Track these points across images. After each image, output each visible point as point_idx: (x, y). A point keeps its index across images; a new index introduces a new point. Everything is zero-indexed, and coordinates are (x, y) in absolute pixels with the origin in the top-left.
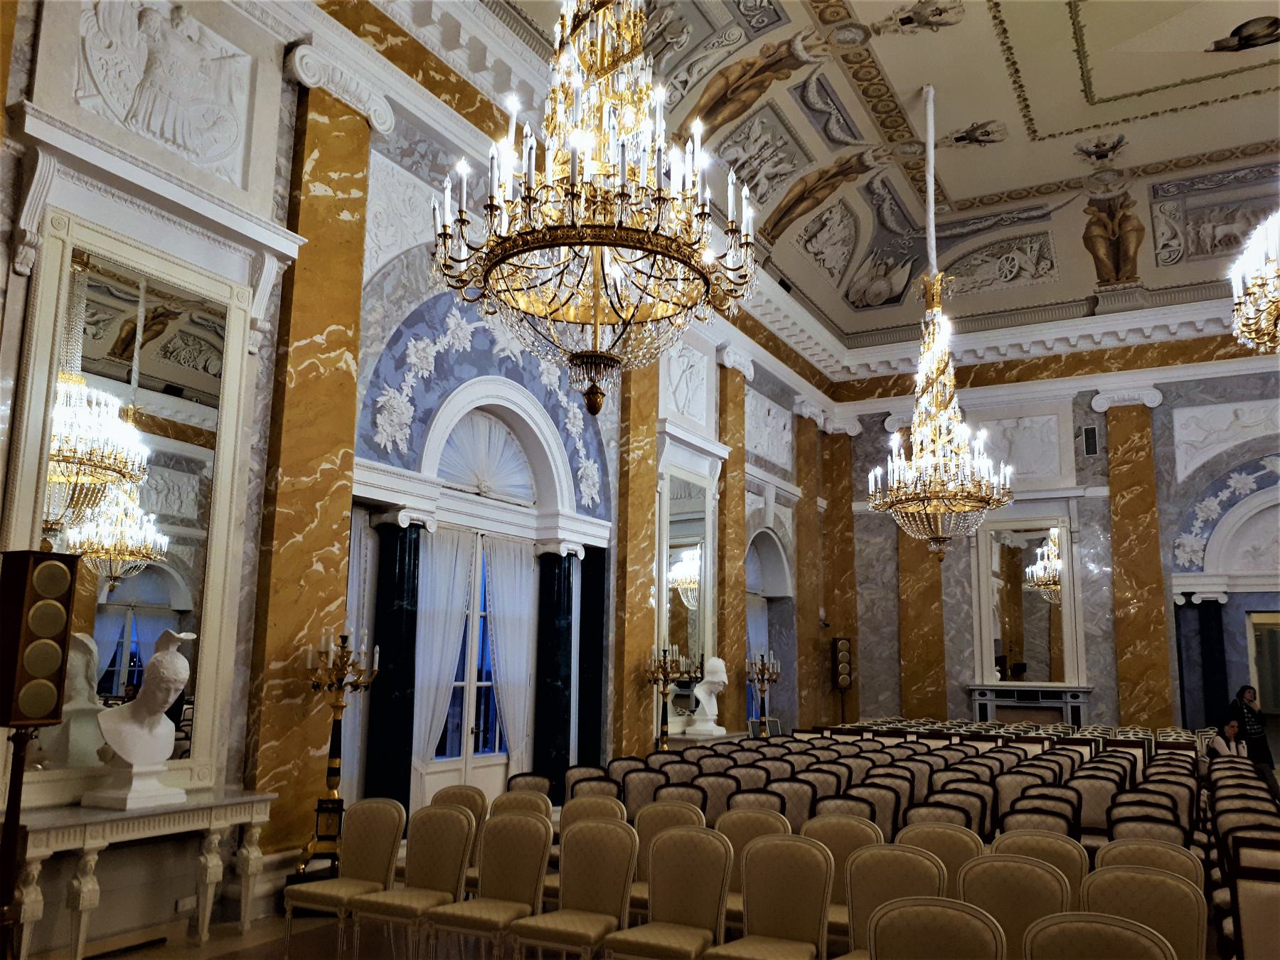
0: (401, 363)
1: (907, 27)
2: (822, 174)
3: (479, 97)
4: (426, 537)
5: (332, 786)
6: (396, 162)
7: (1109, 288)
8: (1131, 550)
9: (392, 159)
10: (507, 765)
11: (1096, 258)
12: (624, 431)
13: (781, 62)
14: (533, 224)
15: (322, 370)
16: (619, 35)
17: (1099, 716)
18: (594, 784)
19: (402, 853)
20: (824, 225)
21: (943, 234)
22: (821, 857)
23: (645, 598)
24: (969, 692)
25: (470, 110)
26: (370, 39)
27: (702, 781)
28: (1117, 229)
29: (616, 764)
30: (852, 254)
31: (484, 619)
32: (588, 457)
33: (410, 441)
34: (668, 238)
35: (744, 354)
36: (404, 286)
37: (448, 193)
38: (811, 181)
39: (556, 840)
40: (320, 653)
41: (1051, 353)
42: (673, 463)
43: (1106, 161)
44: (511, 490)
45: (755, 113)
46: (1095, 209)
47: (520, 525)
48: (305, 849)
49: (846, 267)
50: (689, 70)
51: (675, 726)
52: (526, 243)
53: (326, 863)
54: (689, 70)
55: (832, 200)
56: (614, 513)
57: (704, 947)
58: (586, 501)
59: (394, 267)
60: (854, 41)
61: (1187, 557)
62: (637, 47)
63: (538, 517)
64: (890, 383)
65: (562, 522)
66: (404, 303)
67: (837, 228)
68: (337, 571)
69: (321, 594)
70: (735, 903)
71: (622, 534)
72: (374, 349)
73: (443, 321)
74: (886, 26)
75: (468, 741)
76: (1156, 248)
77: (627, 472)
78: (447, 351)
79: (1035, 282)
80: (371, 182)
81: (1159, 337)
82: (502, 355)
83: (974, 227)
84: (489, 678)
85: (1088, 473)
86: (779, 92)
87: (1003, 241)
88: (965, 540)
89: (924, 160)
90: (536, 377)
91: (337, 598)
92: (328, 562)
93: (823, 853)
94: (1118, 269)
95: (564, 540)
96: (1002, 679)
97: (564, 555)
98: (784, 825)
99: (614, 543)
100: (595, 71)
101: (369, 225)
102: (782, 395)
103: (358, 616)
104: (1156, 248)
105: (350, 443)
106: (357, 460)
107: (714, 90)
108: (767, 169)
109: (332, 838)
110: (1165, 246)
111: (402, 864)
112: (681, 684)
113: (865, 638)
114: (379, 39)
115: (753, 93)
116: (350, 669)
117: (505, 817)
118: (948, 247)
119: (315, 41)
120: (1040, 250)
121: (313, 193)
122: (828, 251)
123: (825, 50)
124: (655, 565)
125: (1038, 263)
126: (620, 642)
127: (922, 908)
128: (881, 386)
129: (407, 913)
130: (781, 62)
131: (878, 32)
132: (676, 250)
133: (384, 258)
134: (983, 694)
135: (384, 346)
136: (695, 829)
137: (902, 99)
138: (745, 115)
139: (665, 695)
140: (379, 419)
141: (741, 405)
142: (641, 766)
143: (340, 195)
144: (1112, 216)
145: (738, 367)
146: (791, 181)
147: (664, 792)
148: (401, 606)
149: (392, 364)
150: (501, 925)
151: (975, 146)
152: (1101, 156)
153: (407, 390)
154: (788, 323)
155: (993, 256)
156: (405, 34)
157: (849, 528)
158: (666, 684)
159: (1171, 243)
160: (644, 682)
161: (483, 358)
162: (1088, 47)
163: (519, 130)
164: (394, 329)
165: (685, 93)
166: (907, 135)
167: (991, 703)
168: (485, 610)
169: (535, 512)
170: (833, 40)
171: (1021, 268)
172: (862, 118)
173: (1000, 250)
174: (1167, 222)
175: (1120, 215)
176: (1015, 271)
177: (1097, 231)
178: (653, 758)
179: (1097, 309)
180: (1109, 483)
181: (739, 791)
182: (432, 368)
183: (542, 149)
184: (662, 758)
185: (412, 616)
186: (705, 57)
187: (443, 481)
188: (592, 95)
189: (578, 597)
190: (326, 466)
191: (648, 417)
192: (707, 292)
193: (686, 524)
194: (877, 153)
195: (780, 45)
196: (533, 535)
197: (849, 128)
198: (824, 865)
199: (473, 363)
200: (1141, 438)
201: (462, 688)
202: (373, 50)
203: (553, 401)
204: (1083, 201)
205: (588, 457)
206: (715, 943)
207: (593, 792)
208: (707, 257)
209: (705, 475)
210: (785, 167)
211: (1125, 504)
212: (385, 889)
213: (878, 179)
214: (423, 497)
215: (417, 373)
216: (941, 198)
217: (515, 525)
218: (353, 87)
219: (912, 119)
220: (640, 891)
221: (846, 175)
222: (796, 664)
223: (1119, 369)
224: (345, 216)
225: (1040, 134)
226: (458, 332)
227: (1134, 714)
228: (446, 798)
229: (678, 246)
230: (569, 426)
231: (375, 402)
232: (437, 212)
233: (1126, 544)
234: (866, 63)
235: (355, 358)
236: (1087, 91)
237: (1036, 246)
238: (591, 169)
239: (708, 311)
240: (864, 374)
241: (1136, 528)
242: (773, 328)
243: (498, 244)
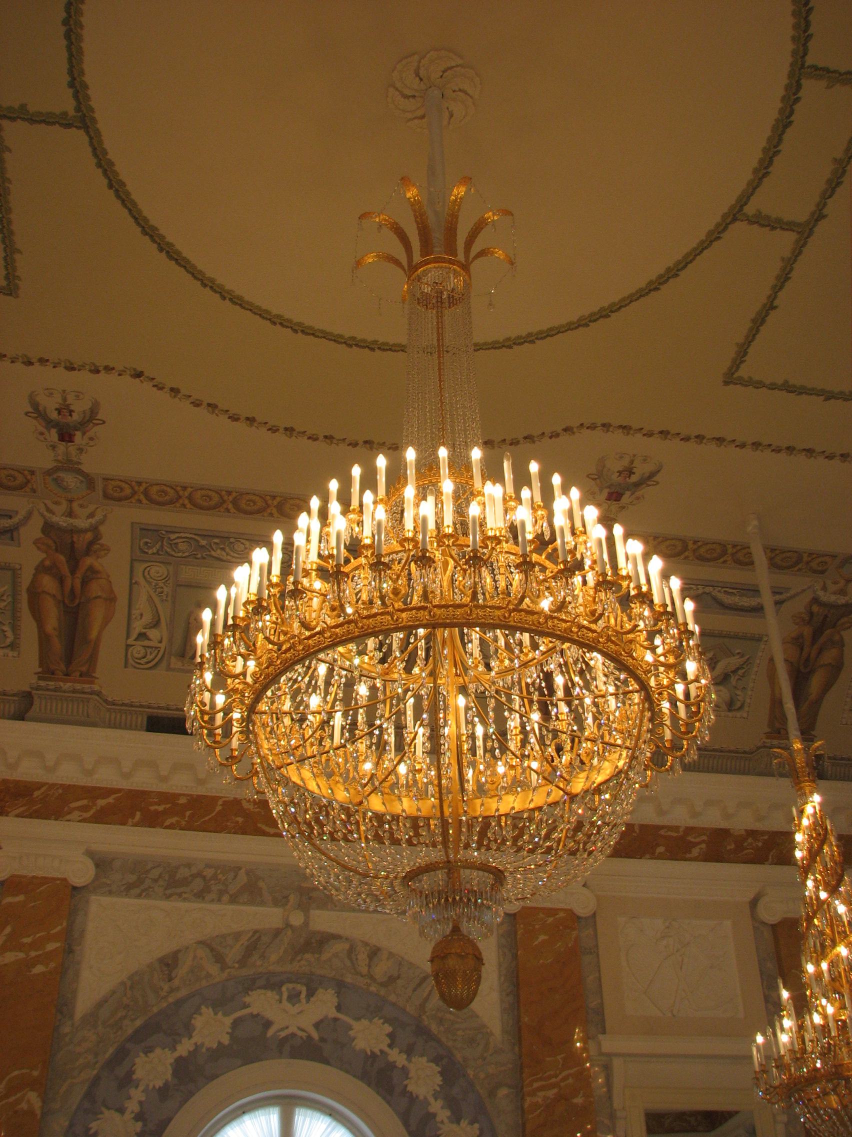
7: (52, 684)
76: (128, 637)
94: (69, 658)
104: (128, 637)
110: (142, 636)
174: (150, 599)
177: (48, 583)
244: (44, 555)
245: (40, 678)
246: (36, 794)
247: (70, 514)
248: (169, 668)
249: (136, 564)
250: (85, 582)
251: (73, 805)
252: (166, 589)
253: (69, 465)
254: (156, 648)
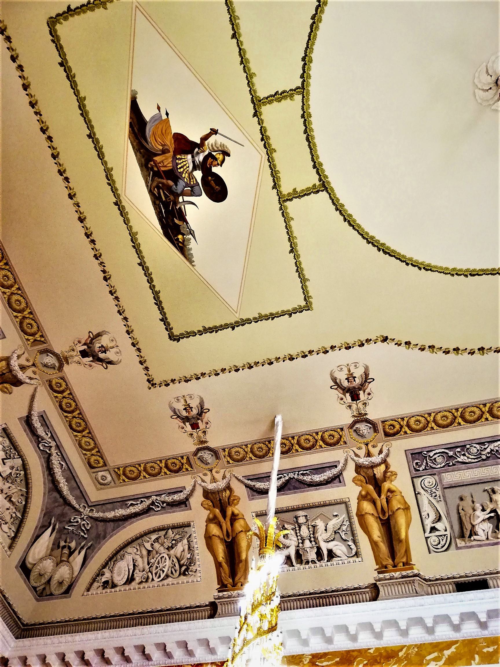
76: (425, 532)
104: (425, 532)
110: (433, 529)
144: (378, 490)
159: (438, 526)
174: (430, 502)
244: (360, 488)
245: (379, 573)
246: (401, 654)
247: (369, 454)
248: (458, 548)
249: (415, 480)
251: (428, 658)
252: (438, 493)
253: (361, 418)
254: (445, 535)
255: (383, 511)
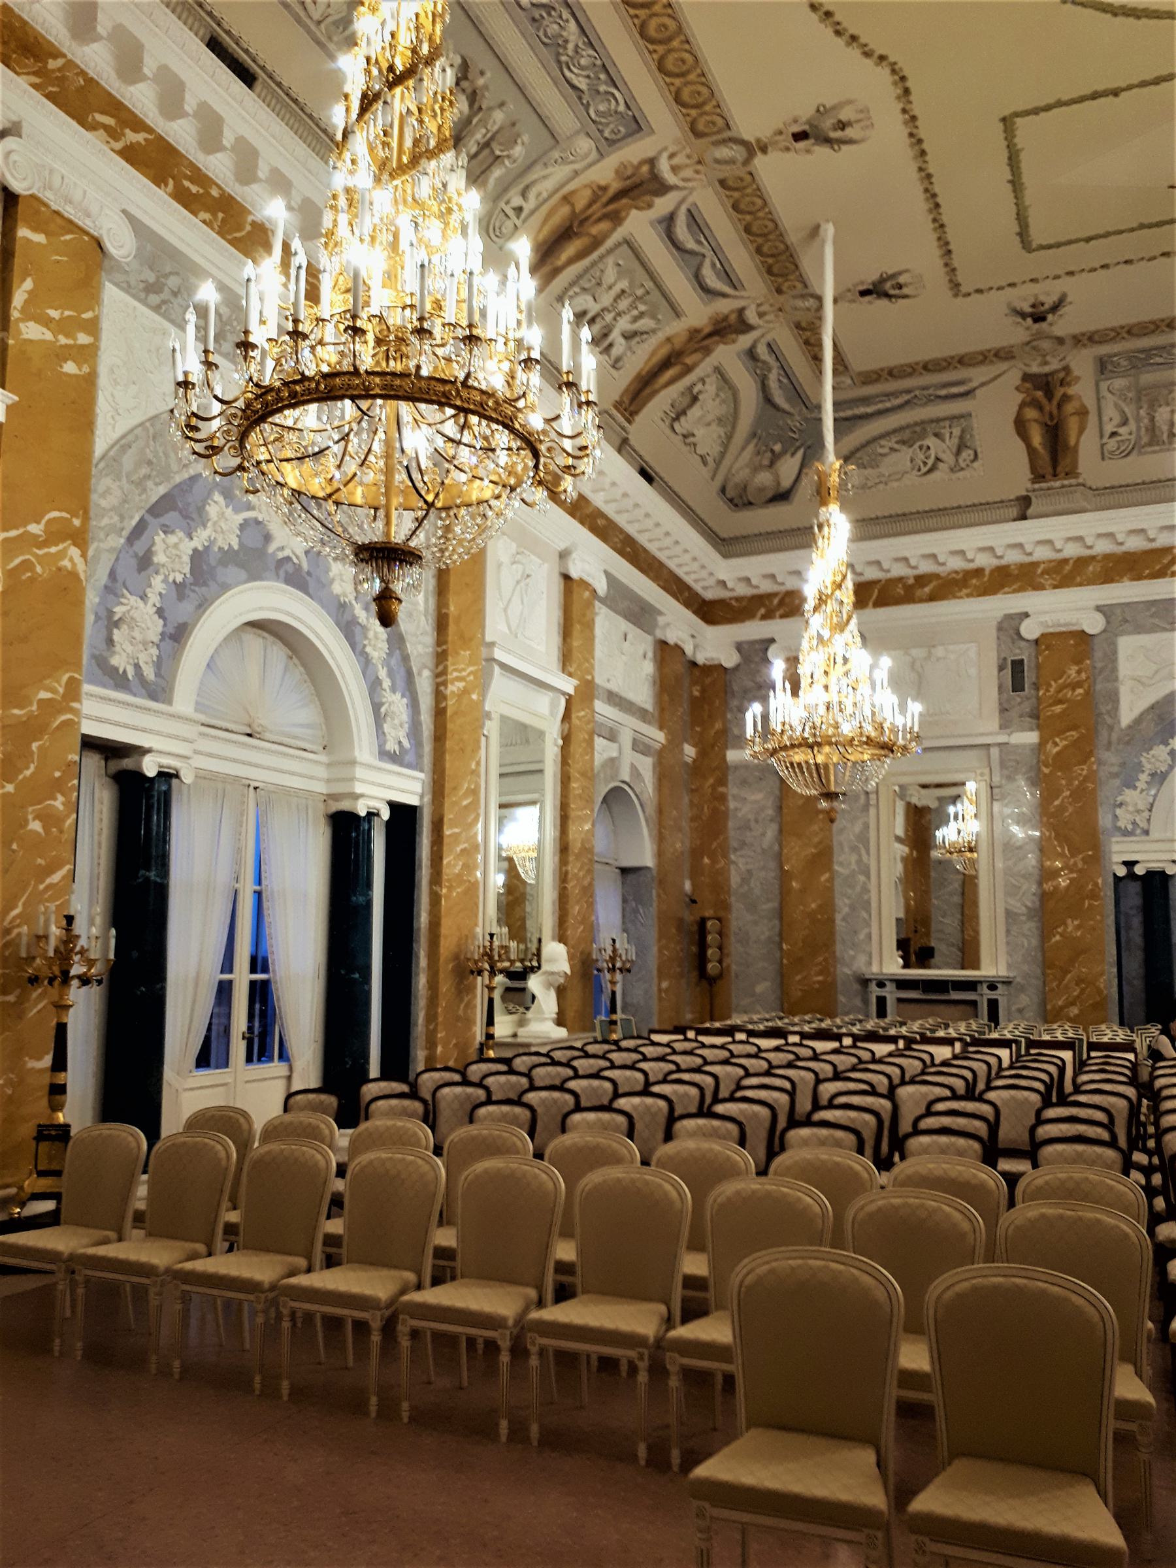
0: (145, 562)
1: (801, 145)
2: (694, 333)
3: (250, 218)
4: (180, 791)
5: (56, 1107)
6: (140, 301)
7: (1044, 485)
8: (1062, 809)
9: (134, 296)
10: (289, 1078)
11: (1029, 446)
12: (441, 657)
13: (642, 186)
14: (302, 368)
15: (39, 569)
16: (421, 122)
17: (1020, 1011)
18: (394, 1102)
19: (142, 1191)
20: (695, 399)
21: (842, 414)
22: (674, 1194)
23: (469, 868)
24: (865, 982)
25: (238, 235)
26: (102, 132)
27: (531, 1097)
28: (1055, 412)
29: (426, 1076)
30: (729, 437)
31: (259, 894)
32: (393, 689)
33: (158, 665)
34: (483, 392)
35: (594, 561)
36: (150, 463)
37: (191, 329)
38: (678, 344)
39: (341, 1171)
40: (39, 938)
41: (971, 566)
42: (503, 699)
43: (1044, 325)
44: (298, 731)
45: (610, 251)
46: (1028, 385)
47: (306, 777)
48: (21, 1188)
49: (723, 454)
50: (524, 194)
51: (503, 1027)
52: (294, 394)
53: (49, 1206)
54: (524, 194)
55: (705, 367)
56: (427, 760)
57: (526, 1310)
58: (391, 746)
59: (137, 437)
60: (732, 161)
61: (1130, 817)
62: (445, 140)
63: (329, 765)
64: (776, 601)
65: (359, 772)
66: (150, 484)
67: (710, 405)
68: (61, 832)
69: (40, 861)
70: (565, 1251)
71: (438, 788)
72: (108, 543)
73: (201, 510)
74: (776, 142)
75: (238, 1048)
76: (1102, 437)
77: (444, 710)
78: (207, 548)
79: (954, 476)
80: (105, 325)
81: (1103, 547)
82: (281, 555)
83: (880, 406)
84: (265, 970)
85: (1014, 713)
86: (639, 224)
87: (916, 424)
88: (863, 797)
89: (820, 318)
90: (325, 584)
91: (60, 867)
92: (48, 818)
93: (675, 1189)
94: (1055, 461)
95: (362, 796)
96: (906, 966)
97: (363, 814)
98: (631, 1152)
99: (427, 799)
100: (386, 170)
101: (103, 381)
102: (640, 614)
103: (91, 890)
104: (1102, 437)
105: (77, 666)
106: (86, 688)
107: (557, 220)
108: (624, 324)
109: (58, 1174)
110: (1114, 434)
111: (141, 1205)
112: (511, 975)
113: (739, 918)
114: (113, 134)
115: (604, 226)
116: (76, 958)
117: (274, 1147)
118: (850, 430)
119: (25, 130)
120: (961, 438)
121: (25, 336)
122: (700, 432)
123: (697, 172)
124: (480, 826)
125: (958, 453)
126: (435, 924)
127: (799, 1262)
128: (763, 605)
129: (145, 1270)
130: (642, 186)
131: (764, 149)
132: (499, 412)
133: (123, 426)
134: (881, 984)
135: (122, 541)
136: (517, 1161)
137: (793, 238)
138: (595, 255)
139: (491, 989)
140: (117, 635)
141: (589, 626)
142: (457, 1077)
143: (63, 340)
144: (1049, 395)
145: (586, 578)
146: (653, 342)
147: (483, 1111)
148: (147, 879)
149: (133, 562)
150: (266, 1286)
151: (884, 302)
152: (1039, 318)
153: (154, 598)
154: (649, 523)
155: (903, 442)
156: (149, 130)
157: (722, 781)
158: (493, 973)
159: (1121, 430)
160: (465, 971)
161: (255, 558)
162: (1026, 178)
163: (286, 247)
164: (137, 519)
165: (518, 223)
166: (799, 285)
167: (891, 994)
168: (260, 883)
169: (323, 758)
170: (708, 158)
171: (938, 459)
172: (742, 260)
173: (911, 435)
174: (1116, 405)
175: (1059, 392)
176: (930, 462)
177: (1031, 414)
178: (474, 1067)
179: (1030, 512)
180: (1039, 727)
181: (578, 1108)
182: (187, 570)
183: (313, 273)
184: (485, 1067)
185: (162, 893)
186: (545, 177)
187: (203, 718)
188: (382, 198)
189: (378, 866)
190: (44, 695)
191: (471, 640)
192: (536, 467)
193: (519, 775)
194: (762, 309)
195: (642, 163)
196: (321, 788)
197: (727, 275)
198: (678, 1204)
199: (242, 565)
200: (1079, 672)
201: (230, 982)
202: (106, 148)
203: (347, 617)
204: (1014, 377)
205: (393, 689)
206: (540, 1304)
207: (392, 1113)
208: (535, 421)
209: (544, 714)
210: (646, 323)
211: (1058, 753)
212: (120, 1240)
213: (764, 341)
214: (176, 737)
215: (166, 577)
216: (841, 368)
217: (300, 775)
218: (77, 196)
219: (806, 263)
220: (445, 1237)
221: (723, 336)
222: (655, 949)
223: (1055, 587)
224: (70, 367)
225: (964, 289)
226: (222, 524)
227: (1062, 1008)
228: (204, 1121)
229: (497, 403)
230: (368, 649)
231: (111, 613)
232: (178, 355)
233: (1057, 803)
234: (749, 191)
235: (84, 555)
236: (1023, 235)
237: (957, 431)
238: (380, 299)
239: (540, 494)
240: (742, 590)
241: (1069, 784)
242: (631, 530)
243: (258, 397)
250: (1059, 406)
255: (1051, 417)
